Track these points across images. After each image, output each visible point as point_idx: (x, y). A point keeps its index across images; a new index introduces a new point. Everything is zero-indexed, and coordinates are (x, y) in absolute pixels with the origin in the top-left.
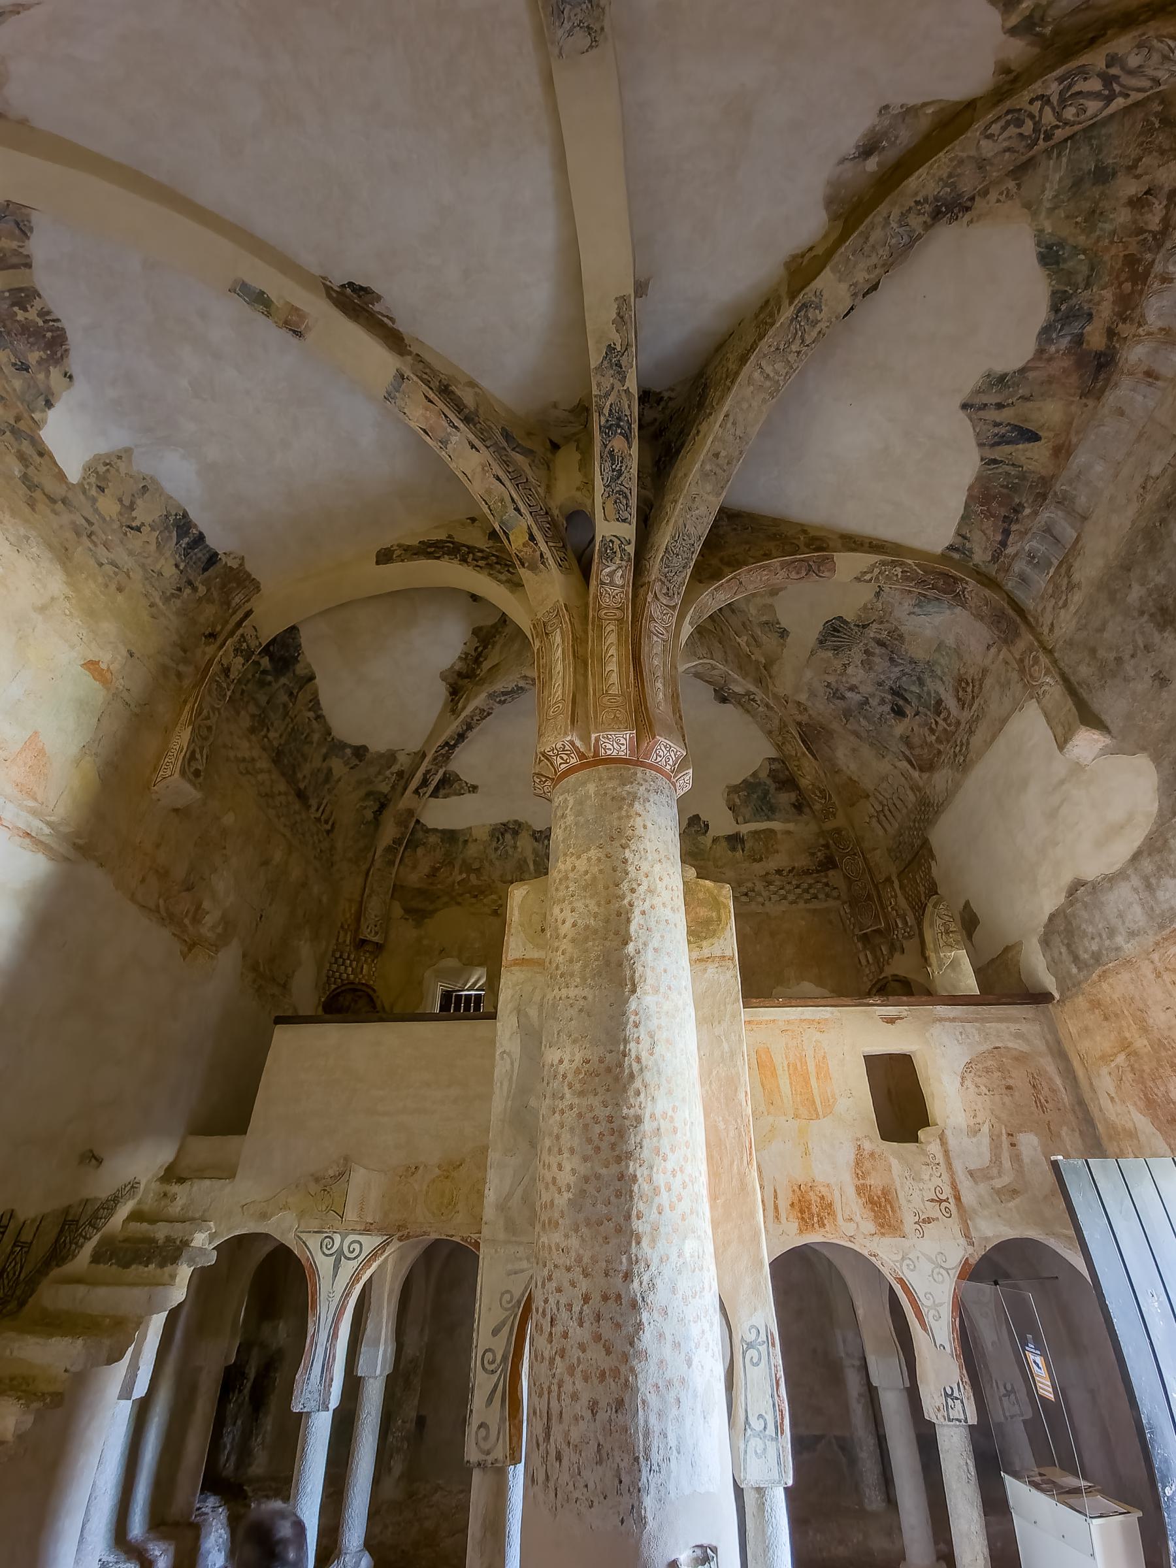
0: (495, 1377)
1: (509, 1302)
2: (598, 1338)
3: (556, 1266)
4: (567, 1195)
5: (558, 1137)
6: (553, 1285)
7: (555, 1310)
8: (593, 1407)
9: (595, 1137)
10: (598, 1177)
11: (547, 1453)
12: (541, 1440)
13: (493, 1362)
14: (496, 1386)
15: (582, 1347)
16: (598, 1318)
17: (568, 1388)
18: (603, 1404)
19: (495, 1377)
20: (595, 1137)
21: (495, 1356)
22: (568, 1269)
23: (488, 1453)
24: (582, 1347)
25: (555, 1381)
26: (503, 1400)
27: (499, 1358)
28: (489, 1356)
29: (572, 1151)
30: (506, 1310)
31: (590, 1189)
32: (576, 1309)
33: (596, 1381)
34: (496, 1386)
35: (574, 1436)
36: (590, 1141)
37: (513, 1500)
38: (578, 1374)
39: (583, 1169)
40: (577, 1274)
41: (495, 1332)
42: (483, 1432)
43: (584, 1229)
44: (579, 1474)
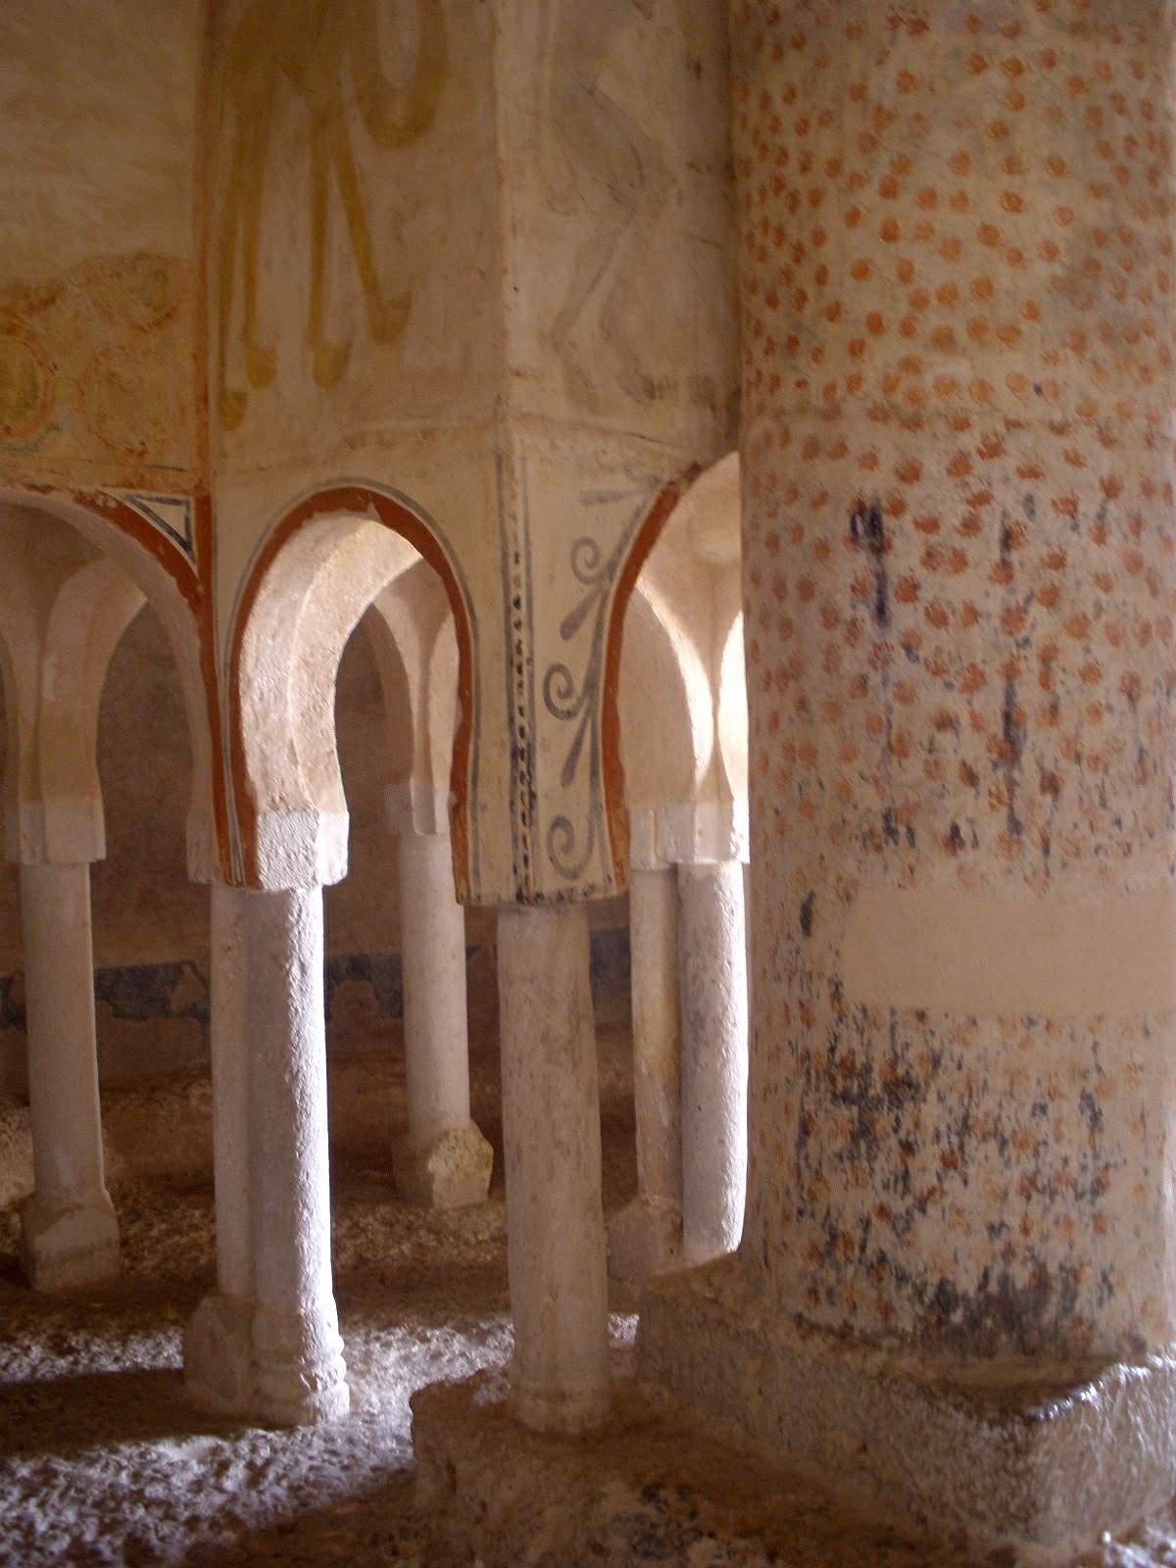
0: (574, 725)
1: (590, 566)
2: (1135, 564)
3: (1013, 425)
4: (1042, 269)
5: (1001, 131)
6: (1011, 462)
7: (1018, 514)
8: (1131, 689)
9: (1118, 146)
10: (1127, 238)
11: (1012, 784)
12: (982, 765)
13: (566, 694)
14: (578, 742)
15: (1104, 583)
16: (1137, 525)
17: (1072, 654)
18: (1147, 682)
19: (574, 725)
20: (1118, 146)
21: (569, 681)
22: (1059, 430)
23: (574, 875)
24: (1104, 583)
25: (1032, 653)
26: (594, 774)
27: (579, 687)
28: (558, 680)
29: (1057, 167)
30: (586, 581)
31: (1108, 259)
32: (1088, 508)
33: (1134, 644)
34: (578, 742)
35: (1092, 740)
36: (1105, 150)
37: (305, 1032)
38: (1097, 630)
39: (1092, 213)
40: (1084, 439)
41: (568, 629)
42: (560, 836)
43: (1098, 349)
44: (1103, 804)
